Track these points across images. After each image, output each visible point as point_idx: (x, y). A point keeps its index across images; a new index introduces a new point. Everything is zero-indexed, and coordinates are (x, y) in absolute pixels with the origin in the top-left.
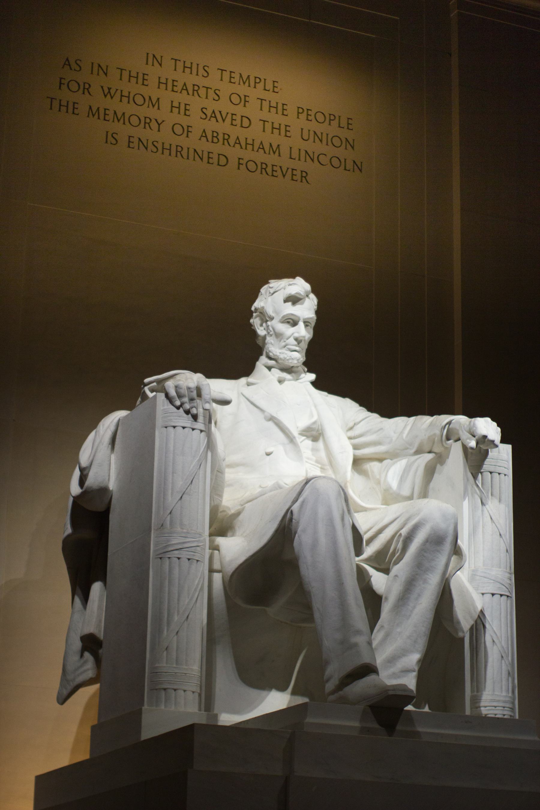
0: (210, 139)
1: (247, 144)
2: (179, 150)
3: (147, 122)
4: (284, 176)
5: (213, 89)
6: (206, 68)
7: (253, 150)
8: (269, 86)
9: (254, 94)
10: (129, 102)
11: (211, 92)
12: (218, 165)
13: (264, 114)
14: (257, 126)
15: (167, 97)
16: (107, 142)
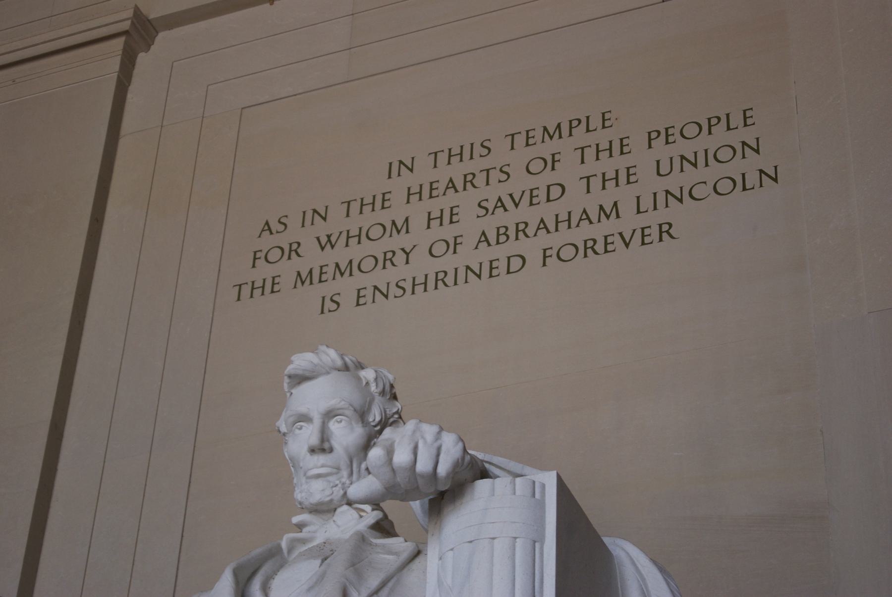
0: (493, 241)
1: (557, 222)
2: (440, 279)
3: (388, 259)
4: (627, 245)
5: (498, 169)
6: (486, 144)
7: (569, 227)
8: (595, 122)
9: (565, 147)
10: (359, 243)
11: (495, 175)
12: (508, 272)
13: (591, 167)
14: (576, 188)
15: (417, 212)
16: (322, 312)
